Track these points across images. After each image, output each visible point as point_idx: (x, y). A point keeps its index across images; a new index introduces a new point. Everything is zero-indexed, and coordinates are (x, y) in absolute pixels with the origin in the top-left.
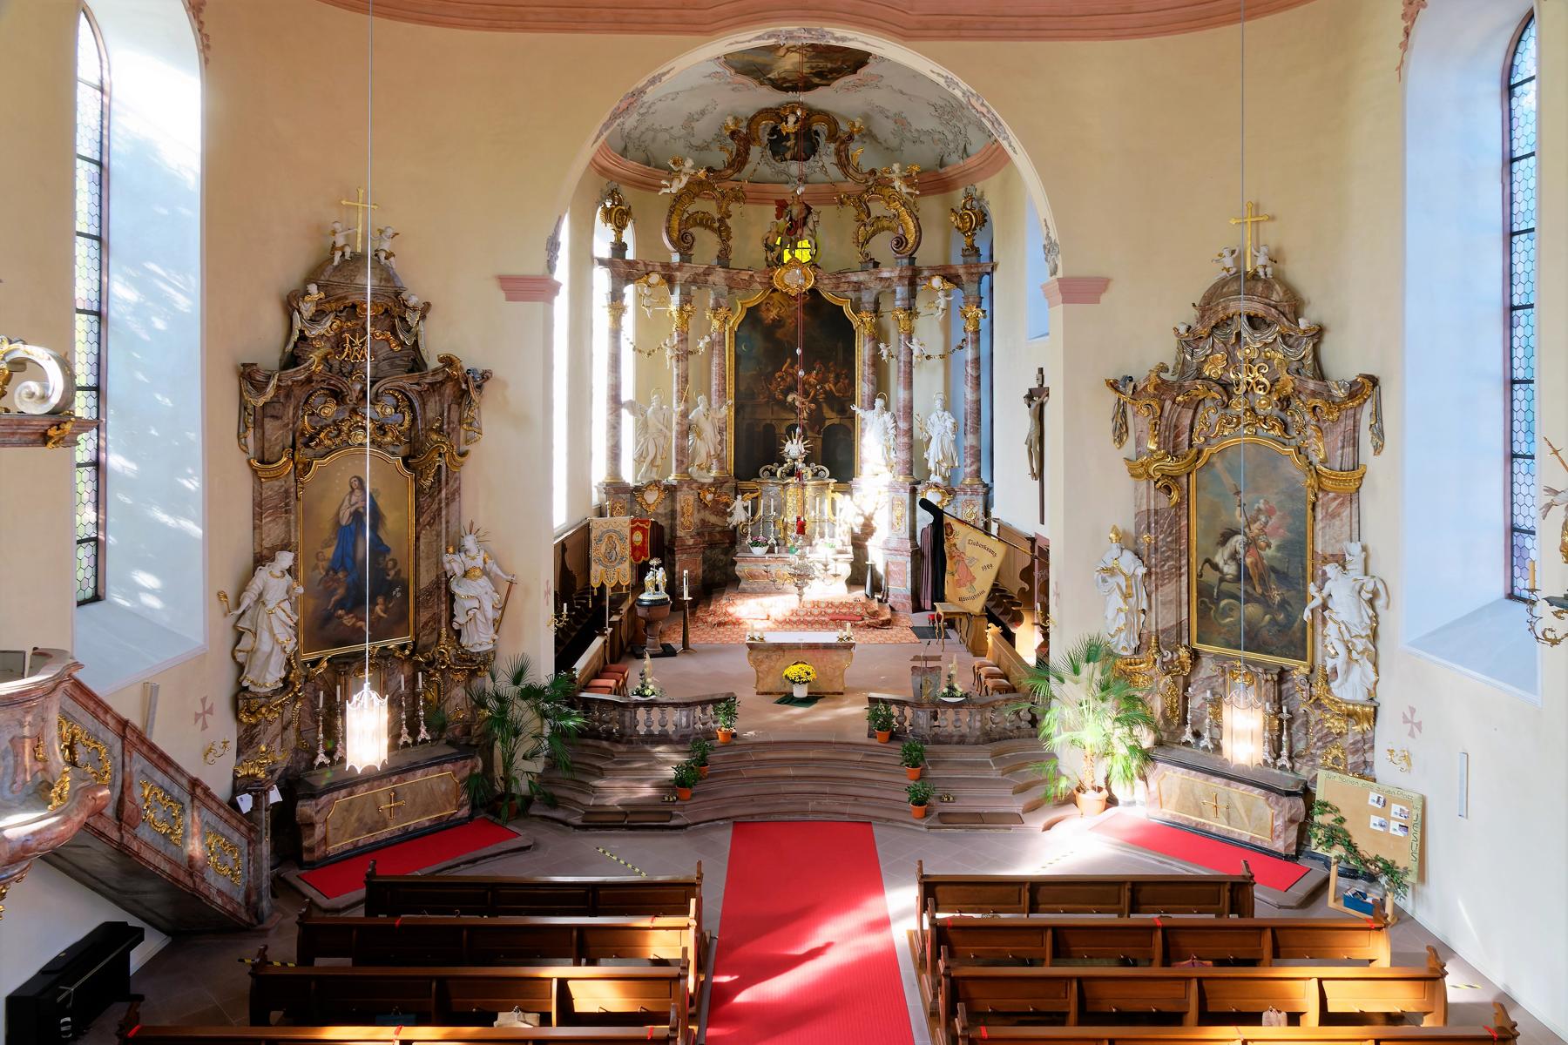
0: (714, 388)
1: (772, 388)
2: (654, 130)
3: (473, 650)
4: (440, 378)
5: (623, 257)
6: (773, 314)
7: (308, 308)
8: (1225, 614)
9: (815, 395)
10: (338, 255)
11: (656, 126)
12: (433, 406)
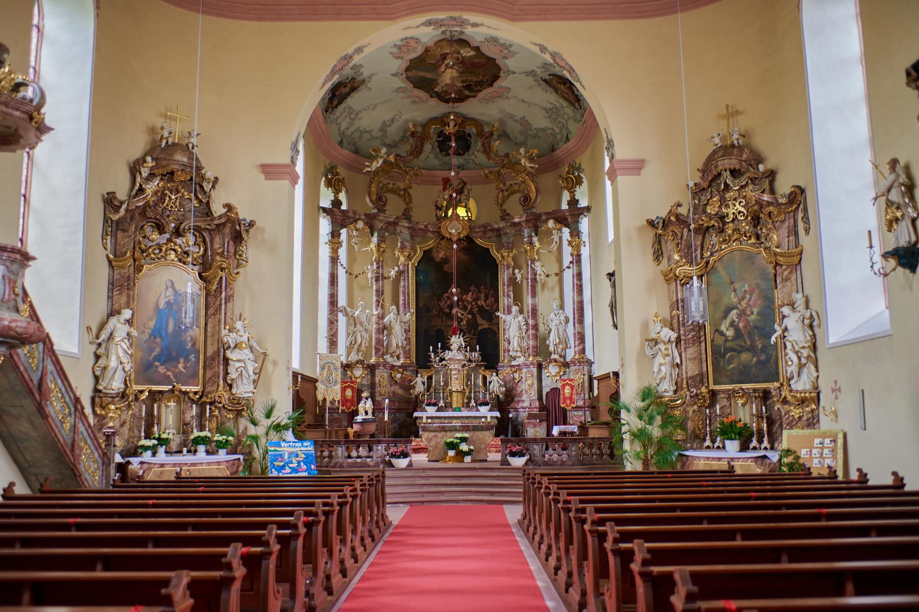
0: (401, 302)
1: (441, 304)
2: (361, 131)
3: (240, 396)
4: (223, 220)
5: (340, 208)
6: (441, 255)
7: (145, 172)
8: (729, 363)
9: (472, 309)
10: (164, 142)
11: (362, 129)
12: (218, 241)
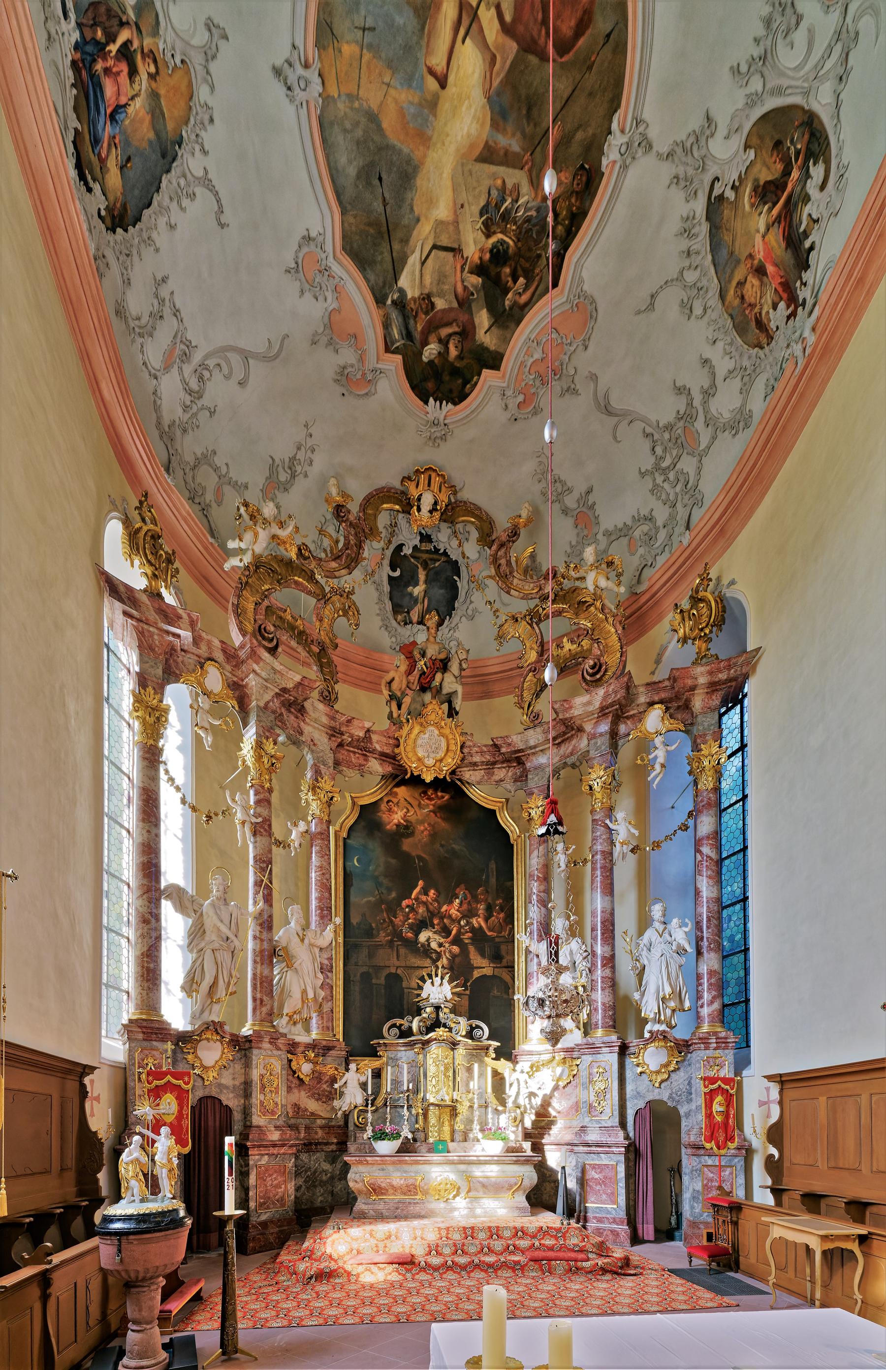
9: (459, 933)
